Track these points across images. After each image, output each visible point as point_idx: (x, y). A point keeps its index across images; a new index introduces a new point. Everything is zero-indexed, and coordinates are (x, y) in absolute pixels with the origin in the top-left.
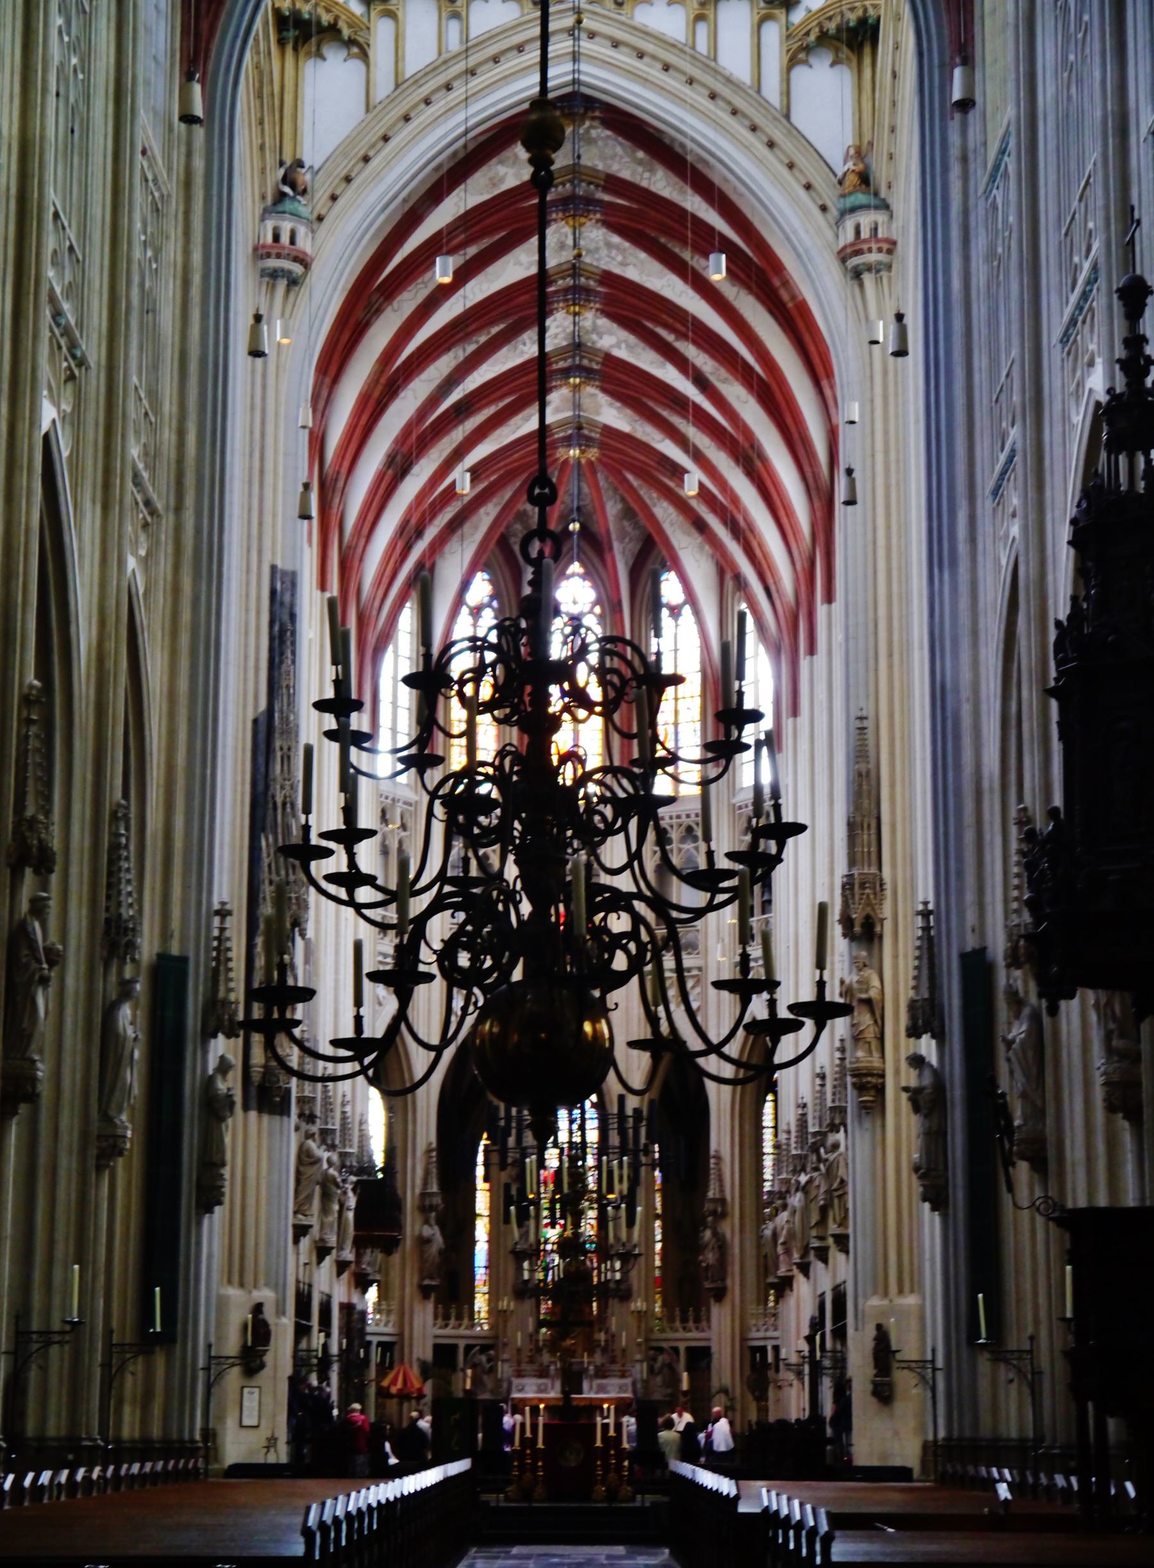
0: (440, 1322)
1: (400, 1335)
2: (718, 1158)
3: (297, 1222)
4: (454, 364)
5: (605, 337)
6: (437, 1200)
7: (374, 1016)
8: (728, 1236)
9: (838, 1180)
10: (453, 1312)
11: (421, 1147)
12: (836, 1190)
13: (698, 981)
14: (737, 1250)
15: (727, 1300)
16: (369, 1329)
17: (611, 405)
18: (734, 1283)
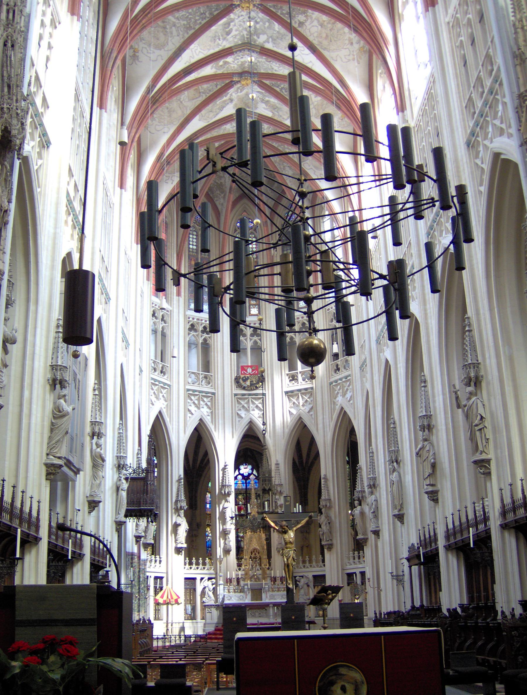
0: (187, 566)
1: (167, 573)
2: (326, 478)
3: (49, 462)
4: (182, 40)
5: (261, 36)
6: (184, 504)
7: (149, 409)
8: (333, 518)
9: (479, 417)
10: (194, 561)
11: (175, 478)
12: (476, 425)
13: (311, 394)
14: (338, 525)
15: (334, 550)
16: (148, 570)
17: (262, 101)
18: (337, 542)
